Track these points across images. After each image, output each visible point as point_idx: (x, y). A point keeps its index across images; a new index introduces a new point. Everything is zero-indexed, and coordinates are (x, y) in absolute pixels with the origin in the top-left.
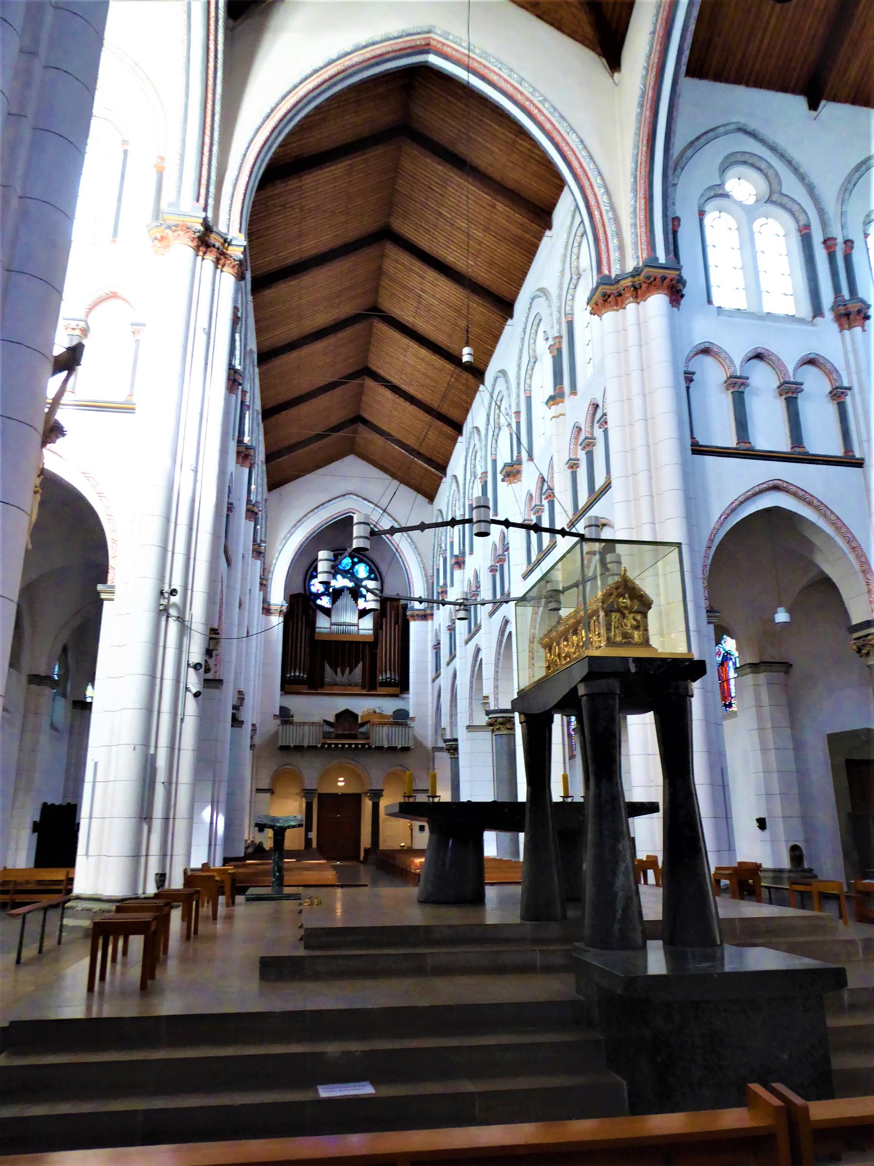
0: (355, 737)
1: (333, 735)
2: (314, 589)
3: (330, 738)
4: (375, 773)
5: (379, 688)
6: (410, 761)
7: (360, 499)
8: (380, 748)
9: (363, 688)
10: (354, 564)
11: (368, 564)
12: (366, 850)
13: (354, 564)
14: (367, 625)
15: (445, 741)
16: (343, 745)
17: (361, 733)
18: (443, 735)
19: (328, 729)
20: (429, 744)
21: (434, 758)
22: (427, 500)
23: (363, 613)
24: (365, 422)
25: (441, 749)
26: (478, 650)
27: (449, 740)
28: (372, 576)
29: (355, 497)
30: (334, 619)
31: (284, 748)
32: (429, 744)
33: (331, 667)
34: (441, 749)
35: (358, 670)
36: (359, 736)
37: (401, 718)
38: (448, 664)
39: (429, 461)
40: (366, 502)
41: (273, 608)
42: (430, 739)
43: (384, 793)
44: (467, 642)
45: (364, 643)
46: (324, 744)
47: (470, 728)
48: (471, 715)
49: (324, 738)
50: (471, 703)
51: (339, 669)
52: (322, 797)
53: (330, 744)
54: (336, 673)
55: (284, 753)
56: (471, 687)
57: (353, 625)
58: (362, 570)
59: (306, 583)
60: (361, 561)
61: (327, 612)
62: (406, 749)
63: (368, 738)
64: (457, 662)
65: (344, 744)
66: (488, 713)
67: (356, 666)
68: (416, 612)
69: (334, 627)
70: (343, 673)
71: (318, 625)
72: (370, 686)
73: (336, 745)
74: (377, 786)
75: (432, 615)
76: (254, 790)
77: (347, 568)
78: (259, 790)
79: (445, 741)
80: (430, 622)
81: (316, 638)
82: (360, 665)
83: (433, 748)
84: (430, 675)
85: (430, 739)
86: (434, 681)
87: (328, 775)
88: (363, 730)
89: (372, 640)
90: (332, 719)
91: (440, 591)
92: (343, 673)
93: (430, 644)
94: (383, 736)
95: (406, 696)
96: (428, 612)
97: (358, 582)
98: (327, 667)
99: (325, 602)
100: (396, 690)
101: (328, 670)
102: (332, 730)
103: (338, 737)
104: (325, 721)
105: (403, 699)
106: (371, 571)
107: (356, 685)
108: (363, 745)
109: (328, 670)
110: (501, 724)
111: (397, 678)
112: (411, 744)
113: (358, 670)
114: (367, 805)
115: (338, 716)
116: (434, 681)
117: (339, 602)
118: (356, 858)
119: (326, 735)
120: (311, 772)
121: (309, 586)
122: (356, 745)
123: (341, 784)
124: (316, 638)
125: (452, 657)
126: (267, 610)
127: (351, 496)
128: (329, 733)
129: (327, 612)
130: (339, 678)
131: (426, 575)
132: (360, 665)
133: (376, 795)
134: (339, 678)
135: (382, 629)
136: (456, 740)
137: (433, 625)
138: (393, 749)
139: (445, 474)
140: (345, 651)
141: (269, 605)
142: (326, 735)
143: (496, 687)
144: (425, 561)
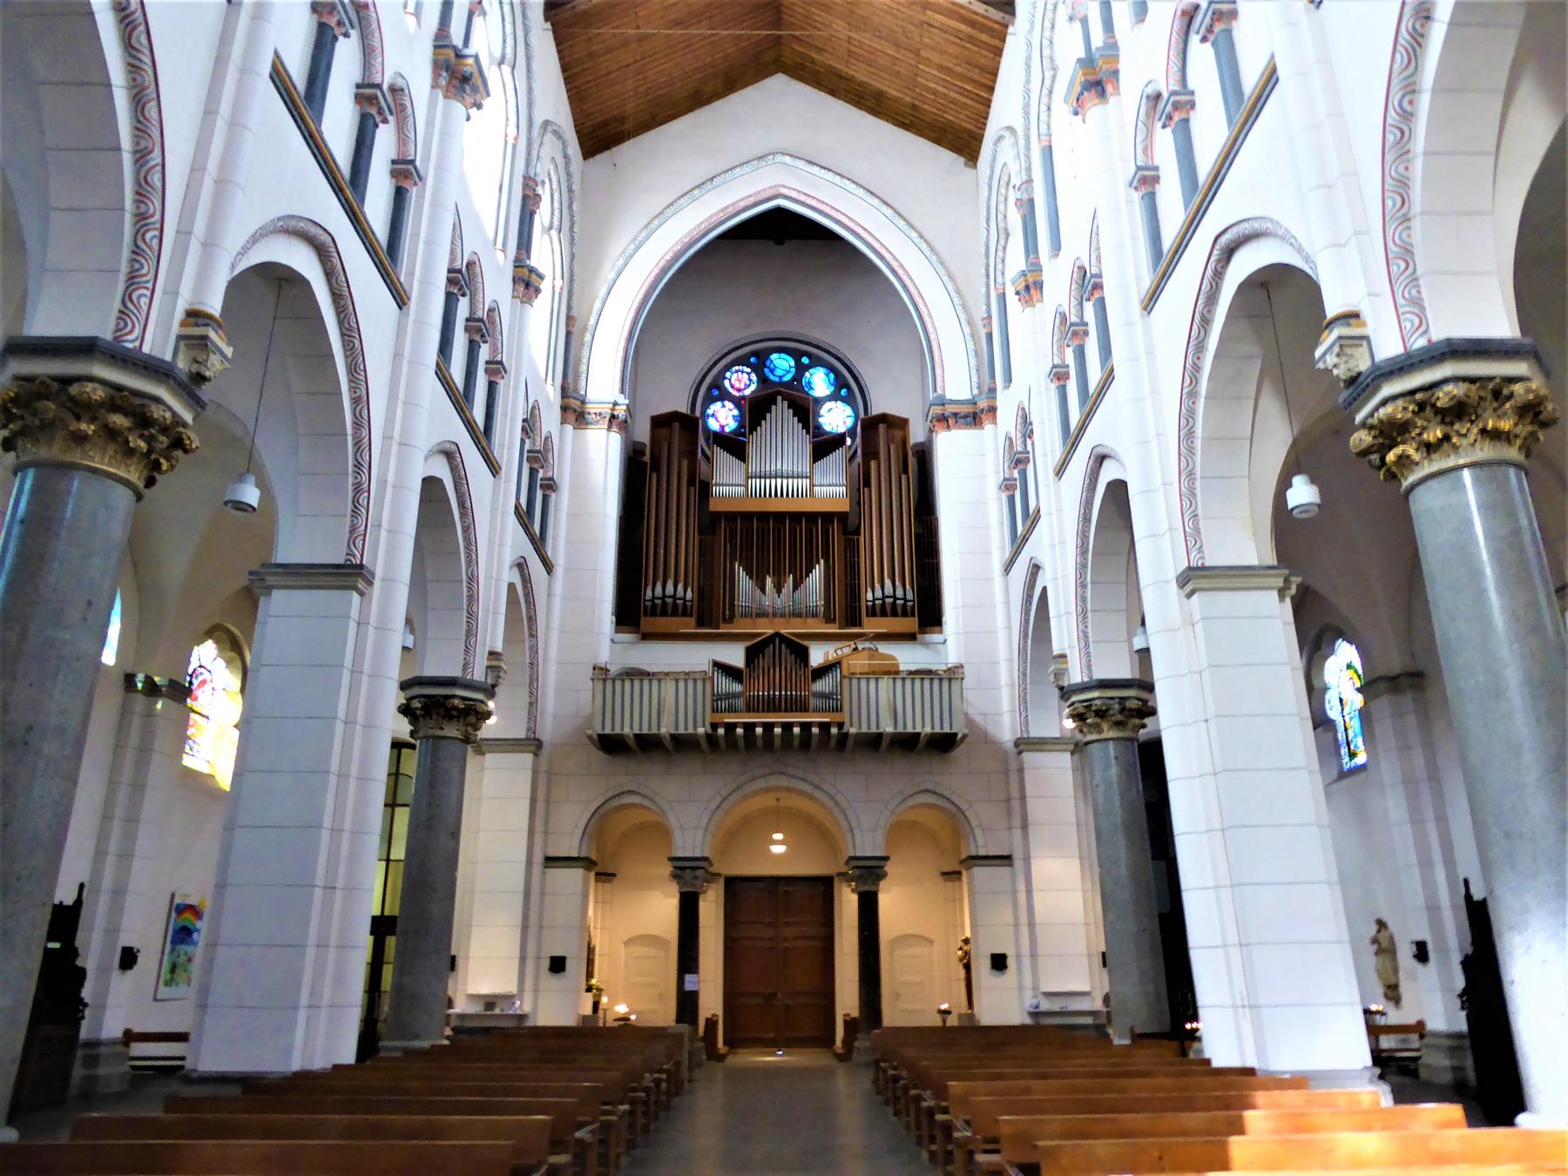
0: (801, 706)
1: (740, 703)
2: (713, 425)
3: (732, 710)
4: (865, 810)
5: (865, 620)
6: (956, 779)
7: (801, 164)
8: (873, 743)
9: (829, 619)
10: (801, 369)
11: (831, 369)
12: (850, 1024)
13: (801, 369)
15: (1065, 693)
17: (822, 695)
18: (1058, 675)
19: (726, 685)
20: (1006, 732)
21: (1021, 770)
22: (962, 160)
25: (1041, 744)
28: (843, 392)
29: (787, 159)
30: (754, 466)
31: (611, 745)
32: (1006, 732)
34: (1041, 744)
35: (817, 576)
36: (813, 702)
40: (815, 170)
41: (591, 408)
42: (1006, 720)
43: (889, 868)
44: (1151, 301)
45: (828, 517)
46: (714, 726)
48: (1193, 536)
49: (715, 710)
50: (1189, 496)
51: (769, 581)
52: (734, 886)
53: (730, 727)
54: (763, 590)
56: (1187, 434)
60: (816, 362)
62: (944, 743)
63: (839, 709)
67: (809, 571)
68: (950, 409)
69: (755, 483)
70: (778, 588)
72: (847, 611)
73: (749, 727)
74: (868, 844)
75: (993, 410)
76: (538, 859)
77: (787, 378)
78: (551, 861)
79: (1065, 693)
80: (988, 427)
81: (714, 506)
82: (817, 573)
83: (1018, 743)
84: (999, 547)
85: (1006, 720)
87: (749, 829)
88: (822, 686)
89: (845, 507)
92: (778, 588)
93: (994, 468)
94: (881, 709)
95: (936, 638)
96: (983, 404)
98: (741, 574)
100: (911, 624)
101: (744, 581)
102: (737, 688)
103: (750, 708)
105: (927, 645)
106: (840, 383)
107: (815, 615)
108: (825, 727)
109: (744, 581)
110: (1459, 412)
111: (910, 596)
112: (959, 729)
113: (817, 576)
114: (847, 902)
118: (827, 1040)
119: (719, 701)
120: (691, 810)
121: (704, 415)
122: (806, 727)
123: (778, 849)
124: (714, 506)
126: (574, 412)
127: (779, 158)
128: (729, 696)
130: (769, 598)
131: (969, 323)
132: (817, 573)
133: (869, 873)
135: (867, 484)
137: (996, 435)
138: (907, 743)
139: (1013, 13)
140: (779, 539)
141: (583, 402)
142: (719, 701)
143: (1401, 257)
144: (964, 290)
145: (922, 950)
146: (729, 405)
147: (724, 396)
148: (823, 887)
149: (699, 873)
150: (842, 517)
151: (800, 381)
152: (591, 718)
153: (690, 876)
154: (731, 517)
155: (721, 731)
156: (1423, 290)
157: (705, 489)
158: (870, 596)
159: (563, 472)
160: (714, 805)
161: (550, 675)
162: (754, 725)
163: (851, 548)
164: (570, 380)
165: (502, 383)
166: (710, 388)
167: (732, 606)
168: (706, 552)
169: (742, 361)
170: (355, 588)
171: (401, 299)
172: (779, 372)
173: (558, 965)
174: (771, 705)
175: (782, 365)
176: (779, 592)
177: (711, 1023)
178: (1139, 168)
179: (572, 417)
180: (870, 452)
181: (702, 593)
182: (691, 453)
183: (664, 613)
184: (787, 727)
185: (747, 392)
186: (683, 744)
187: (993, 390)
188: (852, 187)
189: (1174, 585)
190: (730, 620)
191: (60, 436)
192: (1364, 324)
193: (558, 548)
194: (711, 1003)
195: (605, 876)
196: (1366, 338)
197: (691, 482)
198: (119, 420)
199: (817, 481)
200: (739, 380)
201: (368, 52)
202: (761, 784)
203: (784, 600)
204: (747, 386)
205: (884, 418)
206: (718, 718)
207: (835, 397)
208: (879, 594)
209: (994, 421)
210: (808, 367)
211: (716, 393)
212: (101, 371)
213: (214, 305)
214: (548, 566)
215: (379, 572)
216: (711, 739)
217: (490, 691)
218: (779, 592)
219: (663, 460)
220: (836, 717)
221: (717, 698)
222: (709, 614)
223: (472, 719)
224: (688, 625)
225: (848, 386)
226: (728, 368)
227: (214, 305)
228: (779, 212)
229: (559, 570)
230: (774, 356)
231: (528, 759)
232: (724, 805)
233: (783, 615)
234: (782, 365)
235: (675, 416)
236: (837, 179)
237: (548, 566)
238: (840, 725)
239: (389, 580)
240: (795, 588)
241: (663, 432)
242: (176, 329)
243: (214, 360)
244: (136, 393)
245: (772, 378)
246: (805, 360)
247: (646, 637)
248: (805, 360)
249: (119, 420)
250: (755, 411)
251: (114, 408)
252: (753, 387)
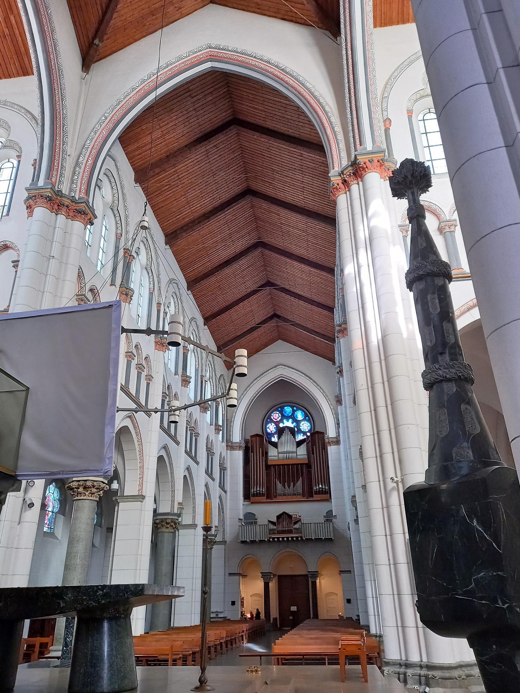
0: (290, 532)
1: (276, 532)
3: (274, 533)
7: (287, 368)
9: (303, 495)
10: (294, 411)
13: (294, 411)
14: (302, 451)
16: (283, 538)
19: (272, 527)
23: (299, 444)
24: (278, 317)
28: (307, 418)
29: (283, 367)
33: (280, 483)
35: (299, 483)
37: (329, 517)
39: (323, 336)
40: (291, 369)
45: (302, 464)
51: (286, 484)
52: (281, 579)
53: (274, 538)
54: (285, 488)
55: (248, 546)
57: (293, 452)
58: (300, 415)
59: (264, 427)
60: (298, 409)
61: (275, 445)
63: (301, 533)
65: (284, 538)
68: (331, 440)
69: (280, 455)
71: (269, 454)
73: (278, 538)
76: (227, 574)
77: (290, 414)
78: (230, 574)
88: (297, 526)
90: (274, 520)
97: (298, 422)
98: (278, 482)
99: (275, 439)
101: (279, 486)
102: (275, 527)
103: (279, 532)
104: (269, 521)
106: (306, 415)
107: (300, 495)
108: (297, 538)
109: (279, 486)
113: (299, 483)
115: (278, 517)
117: (283, 438)
119: (272, 531)
120: (267, 559)
122: (292, 538)
124: (269, 464)
127: (280, 366)
128: (273, 530)
129: (275, 445)
133: (315, 575)
134: (287, 490)
135: (313, 453)
140: (289, 472)
145: (334, 597)
146: (273, 424)
147: (272, 421)
148: (306, 576)
149: (269, 577)
150: (305, 464)
151: (294, 416)
152: (238, 534)
153: (266, 577)
154: (274, 466)
155: (271, 540)
157: (267, 453)
158: (315, 488)
159: (228, 465)
160: (272, 557)
161: (228, 522)
162: (279, 538)
163: (309, 473)
164: (228, 438)
165: (214, 457)
166: (267, 420)
167: (276, 493)
168: (268, 475)
169: (277, 410)
172: (287, 413)
173: (233, 603)
174: (283, 532)
175: (288, 410)
176: (289, 488)
177: (275, 619)
179: (229, 448)
180: (313, 443)
181: (268, 489)
182: (262, 445)
183: (257, 496)
184: (288, 538)
185: (278, 420)
186: (261, 541)
188: (301, 374)
190: (275, 497)
191: (165, 527)
193: (228, 487)
194: (274, 613)
195: (245, 576)
197: (263, 456)
198: (172, 524)
199: (298, 454)
200: (275, 416)
202: (284, 551)
203: (290, 490)
204: (278, 418)
205: (318, 432)
206: (270, 536)
207: (304, 420)
208: (318, 488)
210: (296, 411)
211: (269, 420)
214: (225, 492)
216: (269, 540)
218: (289, 488)
219: (254, 447)
220: (300, 535)
221: (270, 530)
222: (270, 496)
223: (212, 543)
224: (264, 499)
225: (309, 417)
226: (272, 413)
229: (228, 493)
230: (286, 408)
231: (222, 547)
232: (275, 557)
233: (290, 495)
234: (288, 410)
235: (257, 435)
236: (297, 372)
237: (225, 492)
238: (301, 537)
240: (294, 486)
241: (254, 439)
245: (285, 415)
246: (295, 408)
247: (252, 503)
248: (295, 408)
249: (172, 524)
250: (280, 432)
251: (172, 522)
252: (280, 418)
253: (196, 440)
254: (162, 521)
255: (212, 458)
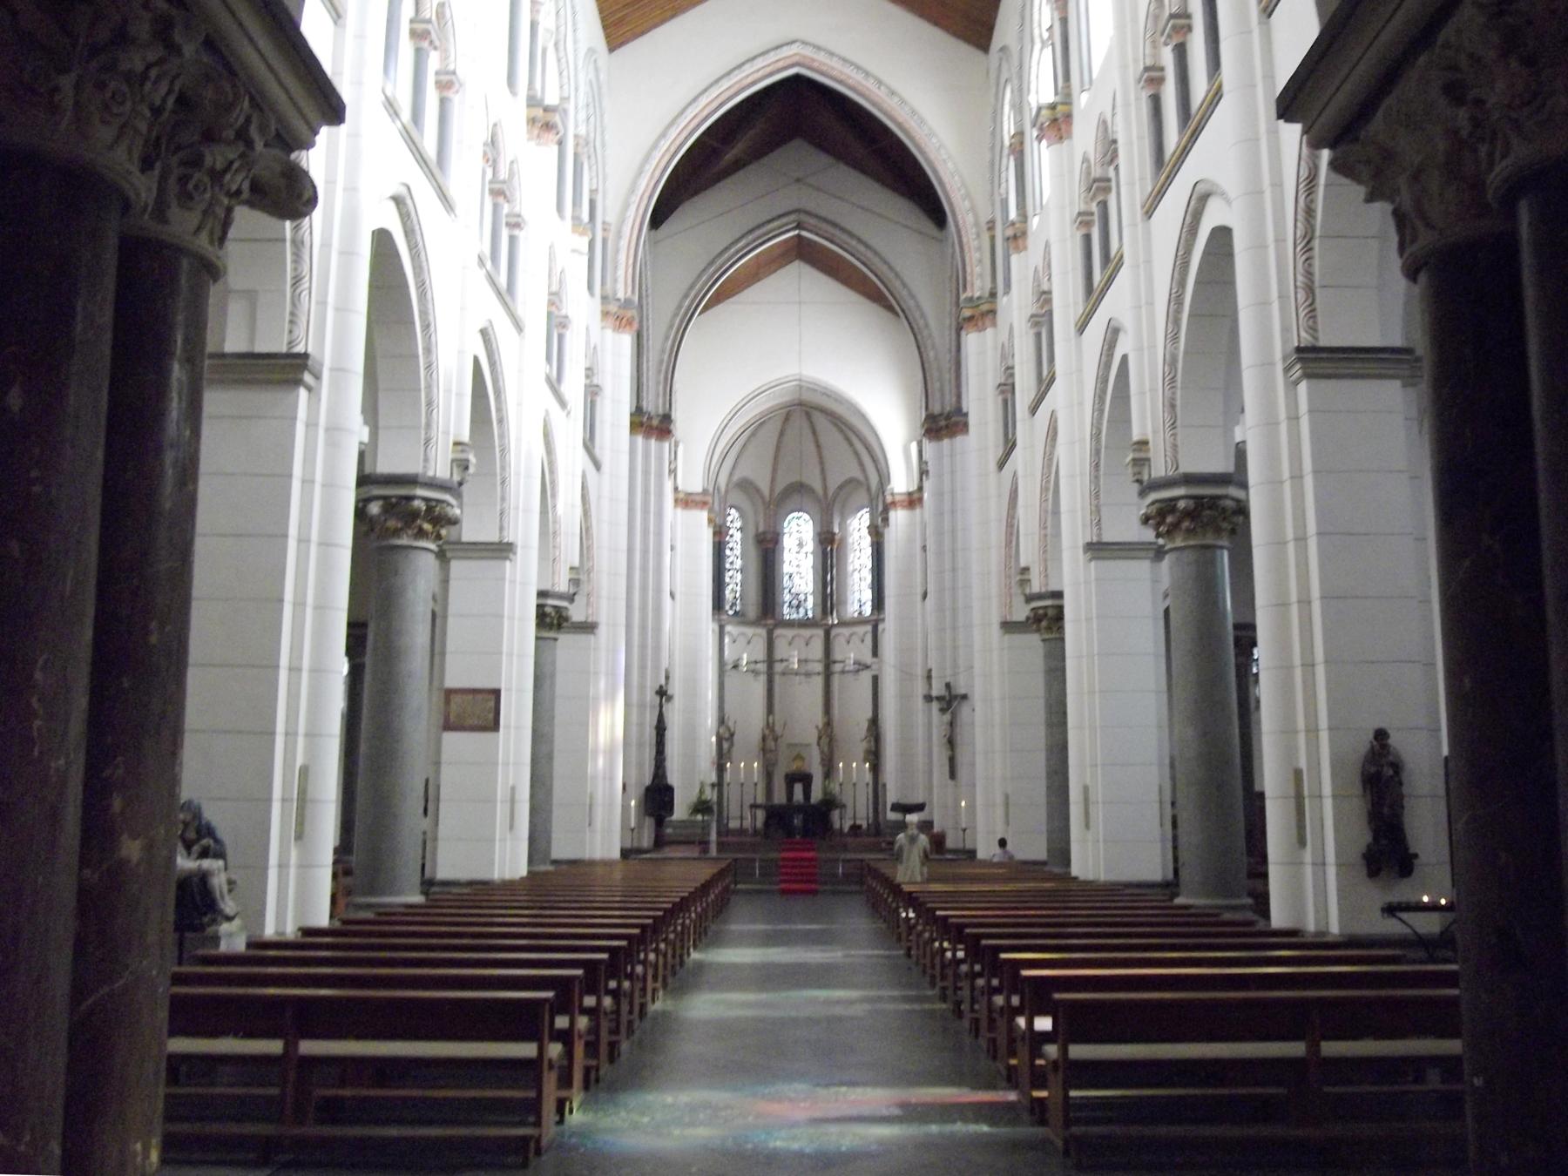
18: (1024, 582)
26: (1113, 333)
27: (1040, 597)
38: (1034, 410)
44: (1081, 329)
47: (1098, 549)
64: (1057, 397)
66: (1146, 488)
75: (993, 312)
79: (1030, 598)
80: (989, 331)
86: (1001, 465)
91: (1010, 232)
96: (985, 308)
116: (1001, 465)
125: (1045, 383)
136: (1058, 595)
156: (1179, 438)
170: (507, 558)
171: (519, 327)
178: (1080, 214)
179: (611, 320)
187: (993, 295)
189: (1081, 551)
192: (1148, 450)
196: (1148, 460)
201: (445, 58)
209: (994, 324)
212: (420, 492)
213: (465, 436)
215: (519, 544)
217: (571, 598)
227: (465, 436)
228: (797, 79)
229: (606, 467)
239: (525, 547)
242: (450, 456)
243: (471, 470)
244: (439, 501)
253: (513, 240)
254: (390, 506)
255: (561, 337)
